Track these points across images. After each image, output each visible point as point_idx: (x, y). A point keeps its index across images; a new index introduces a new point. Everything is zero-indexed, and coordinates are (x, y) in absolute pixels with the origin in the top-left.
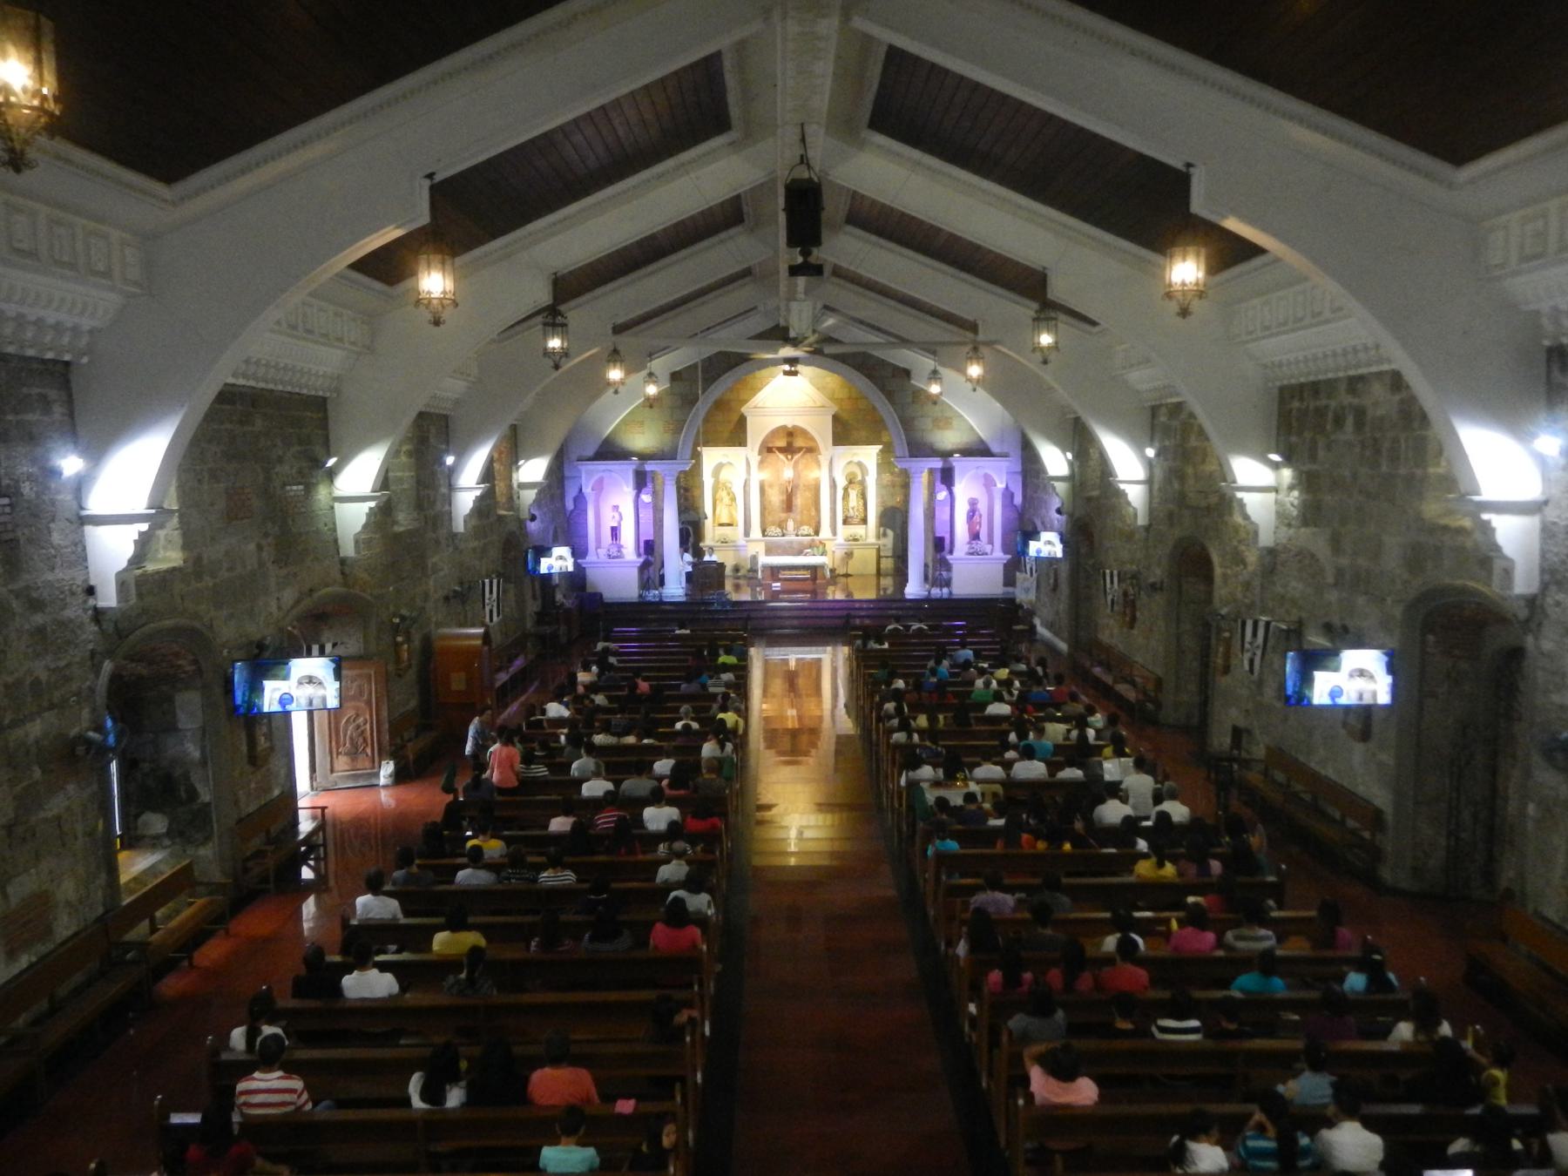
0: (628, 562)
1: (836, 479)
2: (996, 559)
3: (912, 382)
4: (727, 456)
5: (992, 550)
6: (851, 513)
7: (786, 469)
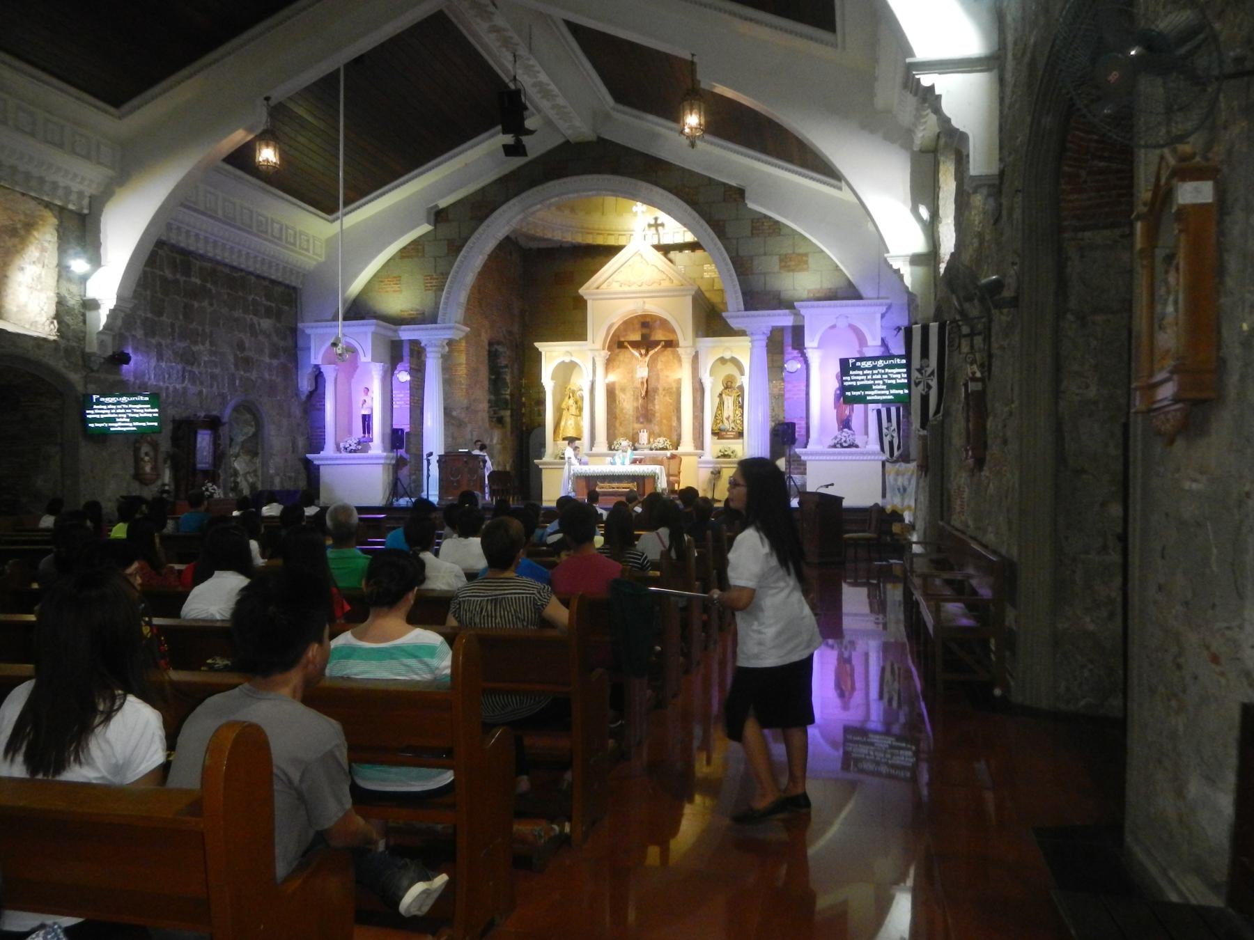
0: (372, 458)
1: (703, 381)
3: (751, 205)
4: (571, 354)
5: (867, 443)
7: (638, 367)
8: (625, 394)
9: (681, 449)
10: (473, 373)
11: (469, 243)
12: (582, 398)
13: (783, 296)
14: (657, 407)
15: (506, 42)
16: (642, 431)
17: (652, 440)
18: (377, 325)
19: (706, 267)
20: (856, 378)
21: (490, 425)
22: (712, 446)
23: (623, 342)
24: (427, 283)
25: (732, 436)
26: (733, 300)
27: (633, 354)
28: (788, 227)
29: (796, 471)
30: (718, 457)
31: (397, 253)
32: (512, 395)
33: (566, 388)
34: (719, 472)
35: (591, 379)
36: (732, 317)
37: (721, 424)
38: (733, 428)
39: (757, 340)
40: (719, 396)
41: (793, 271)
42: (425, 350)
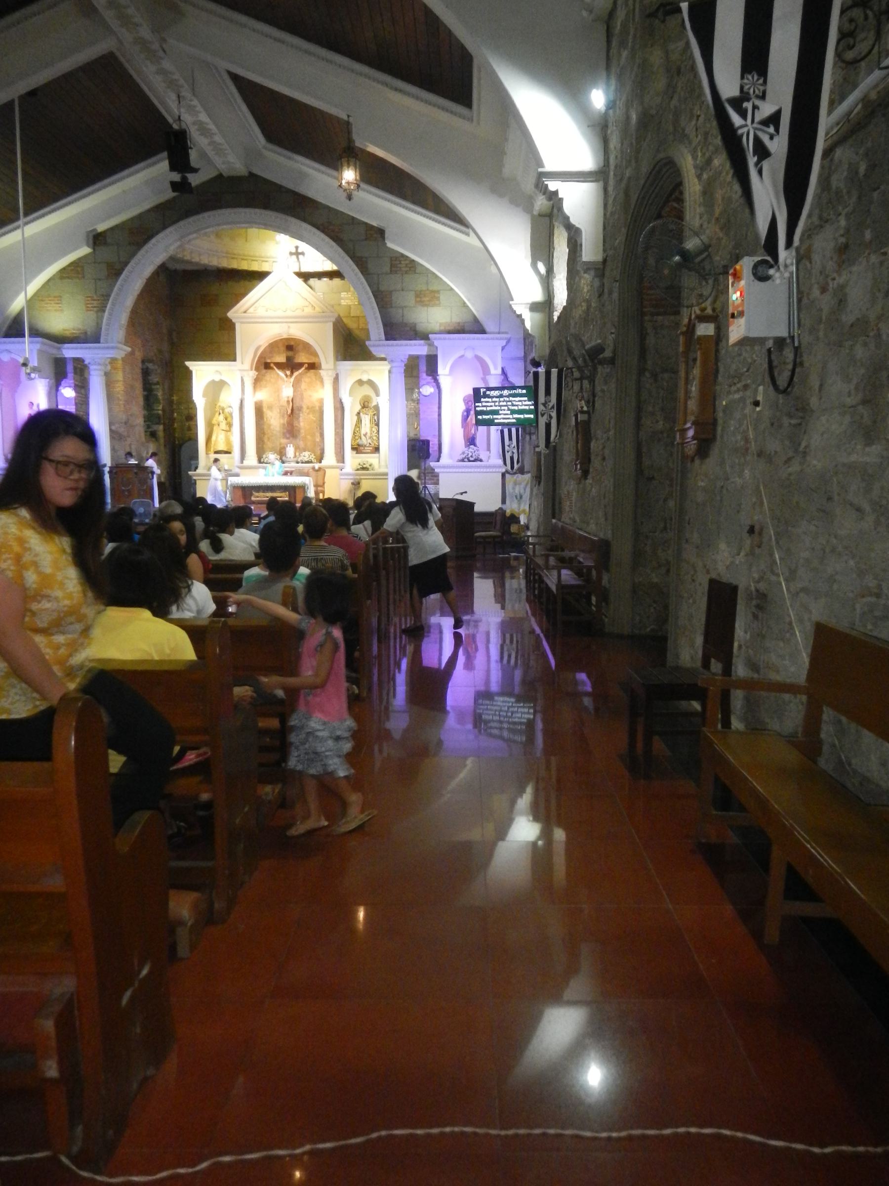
1: (343, 401)
2: (494, 467)
3: (390, 245)
5: (489, 457)
6: (364, 441)
8: (271, 411)
9: (325, 463)
10: (129, 389)
11: (129, 268)
12: (231, 414)
13: (417, 329)
14: (302, 424)
15: (172, 84)
16: (288, 445)
17: (297, 454)
18: (43, 343)
19: (343, 294)
20: (486, 404)
21: (146, 438)
22: (352, 461)
23: (269, 363)
24: (88, 304)
26: (376, 330)
27: (276, 372)
28: (422, 265)
29: (430, 482)
30: (358, 470)
31: (57, 273)
32: (163, 410)
33: (216, 405)
34: (359, 483)
35: (240, 397)
36: (374, 346)
37: (359, 439)
38: (370, 444)
39: (395, 367)
40: (357, 415)
41: (427, 306)
42: (89, 368)
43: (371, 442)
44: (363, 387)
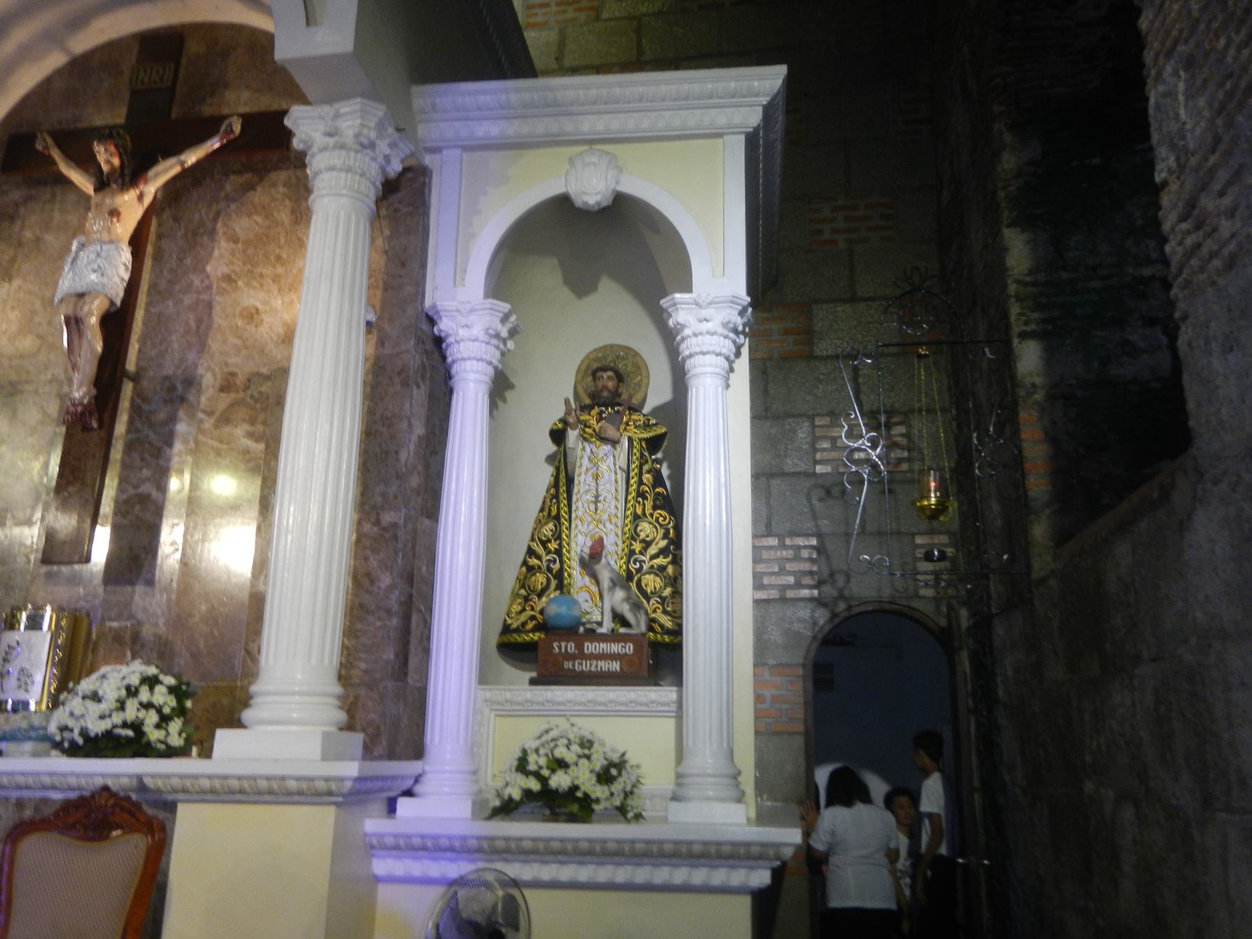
1: (445, 325)
25: (615, 666)
30: (507, 809)
43: (625, 609)
44: (593, 298)
